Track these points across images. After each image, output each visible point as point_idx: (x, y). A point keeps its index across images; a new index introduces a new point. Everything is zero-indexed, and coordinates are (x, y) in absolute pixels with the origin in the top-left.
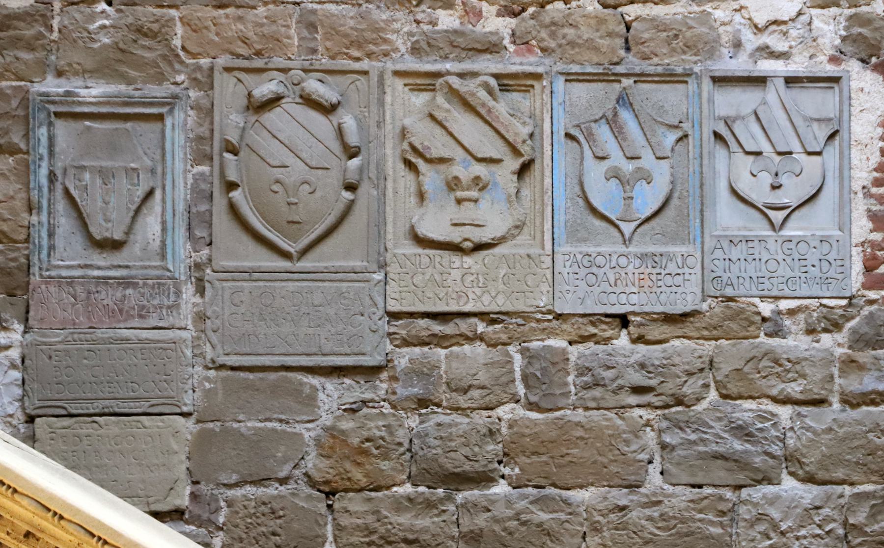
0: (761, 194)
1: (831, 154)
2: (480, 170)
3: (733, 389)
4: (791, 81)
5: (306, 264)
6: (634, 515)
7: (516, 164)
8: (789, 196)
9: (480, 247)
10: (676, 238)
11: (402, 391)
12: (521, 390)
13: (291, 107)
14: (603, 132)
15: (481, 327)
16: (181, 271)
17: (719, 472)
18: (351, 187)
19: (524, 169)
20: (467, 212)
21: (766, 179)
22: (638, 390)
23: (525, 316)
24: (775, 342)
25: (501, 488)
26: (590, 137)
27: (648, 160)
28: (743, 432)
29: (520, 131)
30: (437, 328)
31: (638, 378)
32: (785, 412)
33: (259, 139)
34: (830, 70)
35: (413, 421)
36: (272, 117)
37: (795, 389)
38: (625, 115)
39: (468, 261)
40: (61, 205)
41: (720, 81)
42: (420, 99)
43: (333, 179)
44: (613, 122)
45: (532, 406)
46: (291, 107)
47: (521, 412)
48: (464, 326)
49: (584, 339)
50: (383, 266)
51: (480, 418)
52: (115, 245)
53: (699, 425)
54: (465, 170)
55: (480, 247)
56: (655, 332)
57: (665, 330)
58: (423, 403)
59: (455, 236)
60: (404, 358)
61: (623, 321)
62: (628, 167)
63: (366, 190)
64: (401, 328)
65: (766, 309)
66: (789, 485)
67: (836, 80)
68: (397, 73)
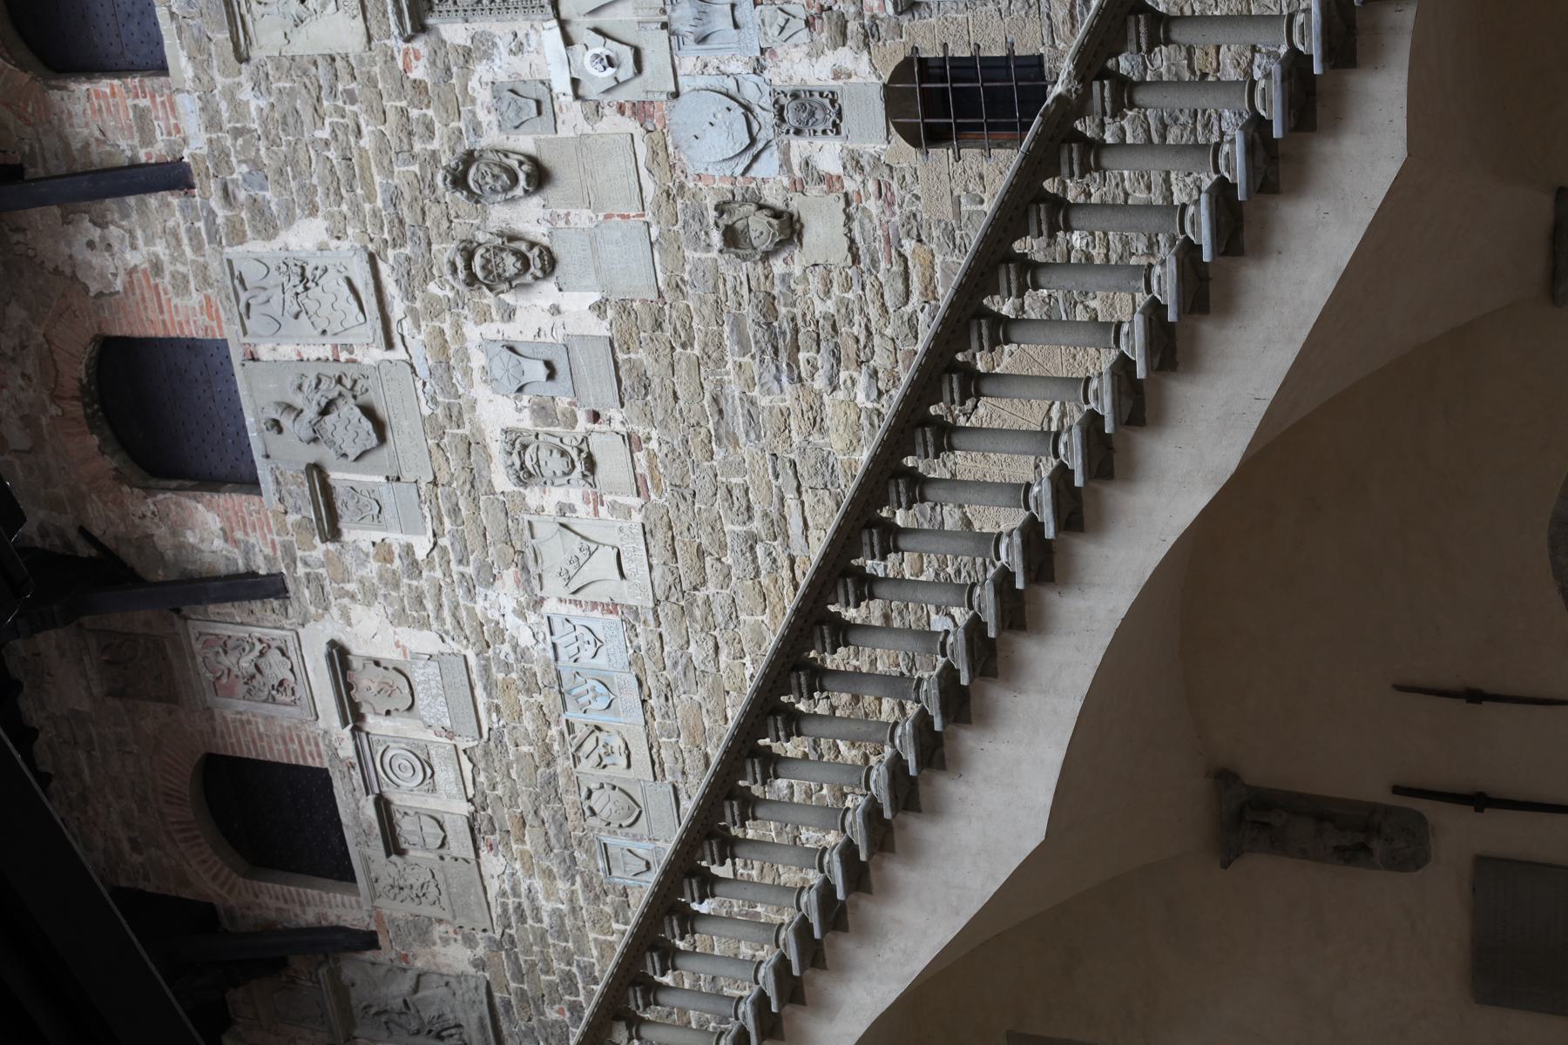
0: (591, 649)
1: (574, 621)
2: (601, 744)
3: (661, 666)
4: (552, 634)
5: (642, 806)
6: (709, 708)
7: (597, 733)
8: (592, 639)
9: (627, 747)
10: (612, 679)
11: (680, 780)
12: (673, 740)
13: (592, 802)
14: (582, 700)
15: (654, 750)
16: (651, 846)
17: (691, 674)
18: (614, 788)
19: (598, 728)
20: (616, 750)
21: (586, 646)
22: (667, 699)
23: (648, 735)
24: (642, 648)
25: (708, 750)
26: (583, 705)
27: (587, 686)
28: (675, 664)
29: (586, 731)
30: (657, 766)
31: (662, 699)
32: (667, 649)
33: (604, 814)
34: (546, 619)
35: (691, 777)
36: (597, 810)
37: (658, 644)
38: (574, 692)
39: (632, 752)
40: (638, 877)
41: (556, 659)
42: (583, 760)
43: (612, 792)
44: (577, 697)
45: (679, 736)
46: (592, 802)
47: (681, 740)
48: (655, 757)
49: (653, 715)
50: (639, 780)
51: (686, 755)
52: (648, 864)
53: (675, 679)
54: (602, 751)
55: (627, 747)
56: (646, 691)
57: (645, 687)
58: (684, 773)
59: (624, 756)
60: (669, 778)
61: (644, 702)
62: (591, 694)
63: (614, 783)
64: (659, 777)
65: (631, 651)
66: (692, 649)
67: (549, 618)
68: (575, 767)
